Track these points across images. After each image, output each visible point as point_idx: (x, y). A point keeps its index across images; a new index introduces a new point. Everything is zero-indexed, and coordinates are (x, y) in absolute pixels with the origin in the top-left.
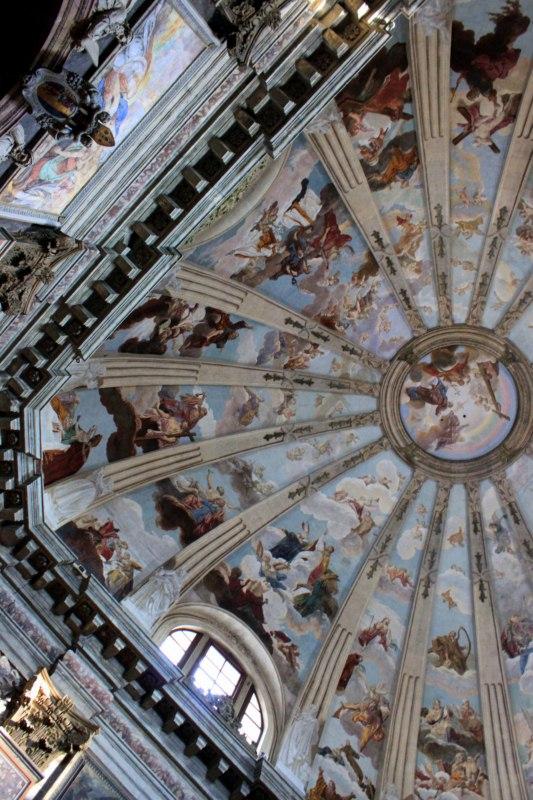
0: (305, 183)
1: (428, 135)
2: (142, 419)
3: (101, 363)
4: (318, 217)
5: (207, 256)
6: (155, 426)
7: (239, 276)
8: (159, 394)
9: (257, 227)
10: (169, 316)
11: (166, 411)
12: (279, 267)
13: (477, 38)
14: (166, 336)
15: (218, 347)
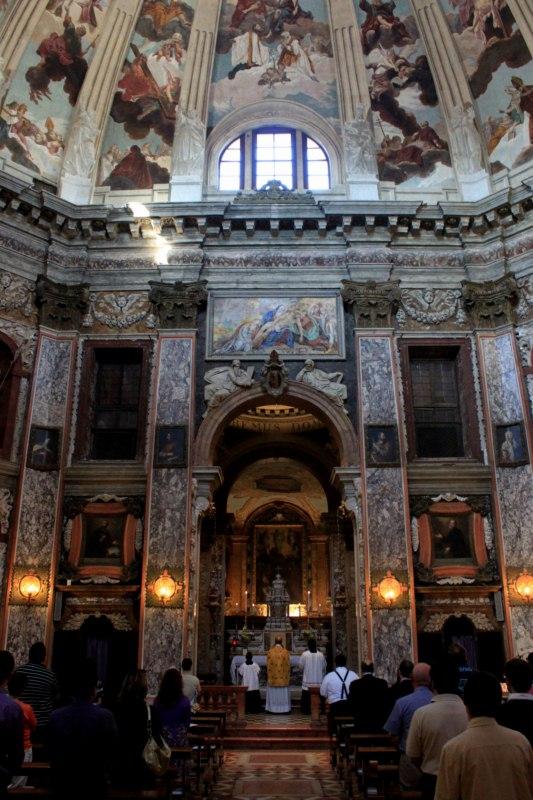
0: (232, 75)
1: (128, 18)
2: (488, 39)
3: (449, 117)
4: (243, 33)
5: (328, 100)
6: (489, 21)
7: (326, 50)
8: (460, 33)
9: (285, 79)
10: (389, 84)
11: (472, 16)
12: (300, 21)
13: (63, 81)
14: (407, 70)
15: (394, 6)
